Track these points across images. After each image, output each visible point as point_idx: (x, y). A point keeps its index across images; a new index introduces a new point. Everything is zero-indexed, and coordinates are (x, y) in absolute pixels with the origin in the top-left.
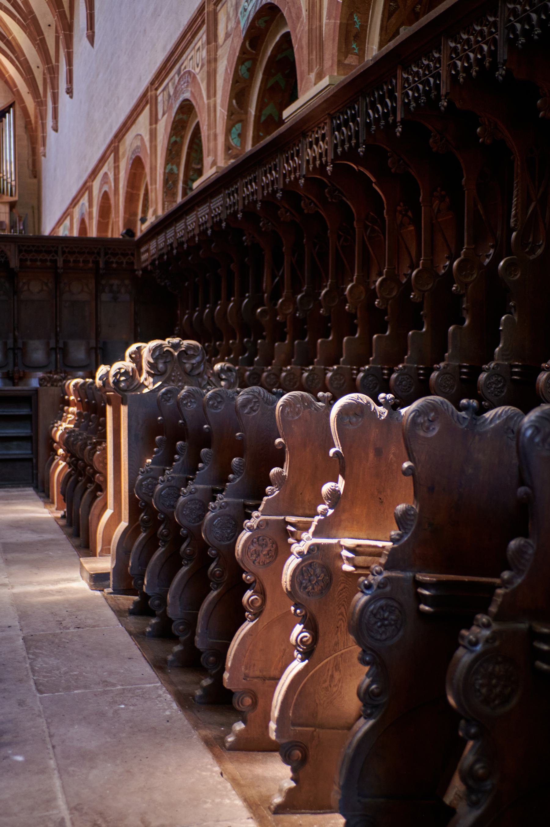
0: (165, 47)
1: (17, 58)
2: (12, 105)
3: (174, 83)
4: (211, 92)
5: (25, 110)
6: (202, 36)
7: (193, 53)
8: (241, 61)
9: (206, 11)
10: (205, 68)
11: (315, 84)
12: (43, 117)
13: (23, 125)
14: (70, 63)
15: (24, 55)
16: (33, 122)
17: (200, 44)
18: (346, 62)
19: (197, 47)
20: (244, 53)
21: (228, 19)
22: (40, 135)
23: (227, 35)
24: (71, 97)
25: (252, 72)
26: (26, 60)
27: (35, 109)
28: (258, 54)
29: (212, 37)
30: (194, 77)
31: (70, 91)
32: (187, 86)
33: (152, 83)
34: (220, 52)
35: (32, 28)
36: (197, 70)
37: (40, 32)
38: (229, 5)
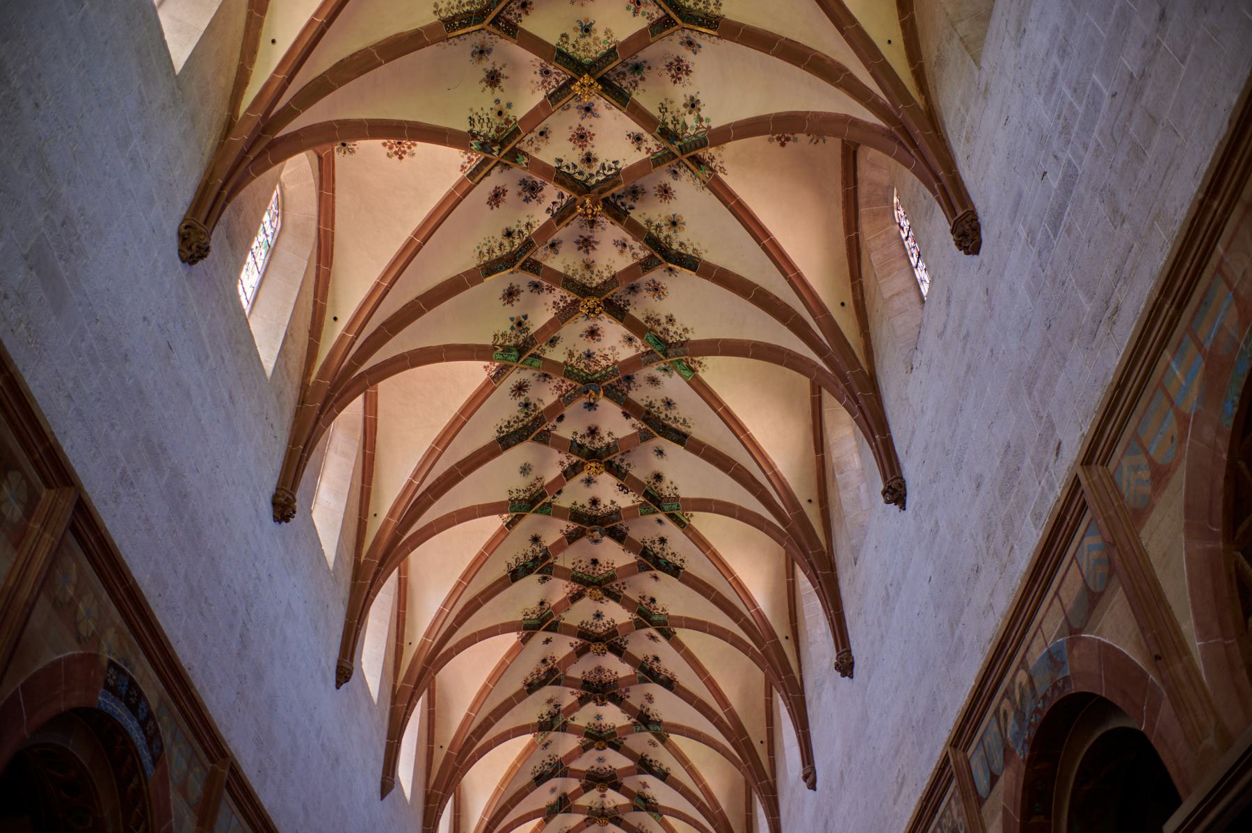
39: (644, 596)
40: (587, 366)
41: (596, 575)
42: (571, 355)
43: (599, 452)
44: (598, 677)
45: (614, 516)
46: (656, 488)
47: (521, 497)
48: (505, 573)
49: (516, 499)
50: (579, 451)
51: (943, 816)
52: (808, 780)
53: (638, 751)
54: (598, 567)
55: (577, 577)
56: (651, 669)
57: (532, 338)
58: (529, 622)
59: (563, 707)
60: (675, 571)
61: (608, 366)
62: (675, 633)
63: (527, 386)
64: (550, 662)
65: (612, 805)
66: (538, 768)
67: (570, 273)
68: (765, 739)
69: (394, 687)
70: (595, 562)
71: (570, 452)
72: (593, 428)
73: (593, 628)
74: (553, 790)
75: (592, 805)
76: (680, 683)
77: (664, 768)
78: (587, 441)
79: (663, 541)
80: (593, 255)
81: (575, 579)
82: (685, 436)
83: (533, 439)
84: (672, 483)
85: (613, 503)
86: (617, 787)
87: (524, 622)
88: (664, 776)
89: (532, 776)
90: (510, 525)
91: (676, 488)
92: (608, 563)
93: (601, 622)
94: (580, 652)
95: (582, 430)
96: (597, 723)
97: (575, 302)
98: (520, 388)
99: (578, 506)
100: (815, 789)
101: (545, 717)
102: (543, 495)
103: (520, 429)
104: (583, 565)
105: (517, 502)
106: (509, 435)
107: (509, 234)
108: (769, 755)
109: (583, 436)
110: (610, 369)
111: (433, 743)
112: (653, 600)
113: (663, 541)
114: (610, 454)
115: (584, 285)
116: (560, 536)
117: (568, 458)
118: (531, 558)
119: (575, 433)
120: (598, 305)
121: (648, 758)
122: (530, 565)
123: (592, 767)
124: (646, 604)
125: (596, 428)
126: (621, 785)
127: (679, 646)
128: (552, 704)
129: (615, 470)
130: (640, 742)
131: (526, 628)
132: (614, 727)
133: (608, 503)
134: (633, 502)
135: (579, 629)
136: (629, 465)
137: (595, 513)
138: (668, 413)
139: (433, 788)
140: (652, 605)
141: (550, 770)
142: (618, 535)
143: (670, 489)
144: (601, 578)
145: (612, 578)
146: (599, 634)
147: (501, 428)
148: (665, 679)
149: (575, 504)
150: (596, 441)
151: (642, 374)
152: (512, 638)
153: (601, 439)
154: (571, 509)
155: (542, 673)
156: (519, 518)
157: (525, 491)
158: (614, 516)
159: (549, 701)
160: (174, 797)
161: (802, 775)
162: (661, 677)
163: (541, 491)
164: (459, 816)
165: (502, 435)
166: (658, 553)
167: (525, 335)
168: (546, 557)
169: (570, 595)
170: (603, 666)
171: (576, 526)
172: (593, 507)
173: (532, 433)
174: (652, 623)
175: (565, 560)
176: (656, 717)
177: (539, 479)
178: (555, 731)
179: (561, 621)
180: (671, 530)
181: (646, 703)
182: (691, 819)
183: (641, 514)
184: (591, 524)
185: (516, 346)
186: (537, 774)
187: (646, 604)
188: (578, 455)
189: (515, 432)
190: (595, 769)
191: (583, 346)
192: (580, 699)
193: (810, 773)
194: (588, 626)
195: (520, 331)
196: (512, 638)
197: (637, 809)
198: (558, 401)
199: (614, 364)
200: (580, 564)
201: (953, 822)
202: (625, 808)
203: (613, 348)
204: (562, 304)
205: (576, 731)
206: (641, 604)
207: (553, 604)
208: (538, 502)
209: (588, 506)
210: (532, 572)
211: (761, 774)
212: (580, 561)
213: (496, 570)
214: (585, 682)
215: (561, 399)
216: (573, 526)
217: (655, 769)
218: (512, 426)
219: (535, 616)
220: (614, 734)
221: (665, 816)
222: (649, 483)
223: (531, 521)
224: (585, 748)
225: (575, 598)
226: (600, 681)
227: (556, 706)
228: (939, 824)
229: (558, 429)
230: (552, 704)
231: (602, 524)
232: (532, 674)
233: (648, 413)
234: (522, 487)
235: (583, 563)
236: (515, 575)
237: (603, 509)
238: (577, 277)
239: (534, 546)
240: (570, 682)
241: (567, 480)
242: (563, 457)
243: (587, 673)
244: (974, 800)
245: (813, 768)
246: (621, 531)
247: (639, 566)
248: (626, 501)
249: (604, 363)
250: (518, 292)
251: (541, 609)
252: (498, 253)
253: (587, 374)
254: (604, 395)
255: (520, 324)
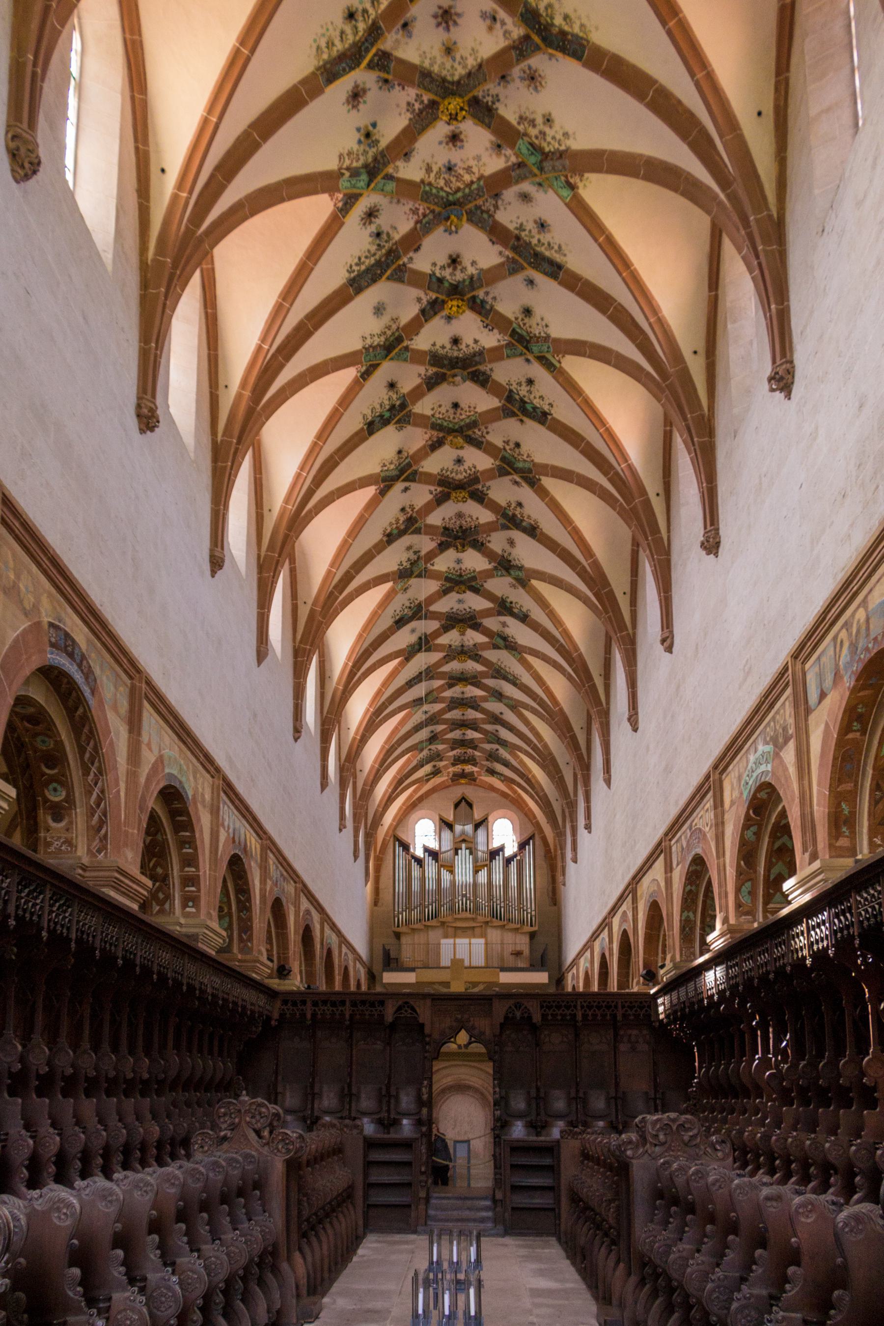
0: (677, 802)
1: (535, 793)
2: (532, 837)
3: (686, 837)
4: (720, 852)
5: (544, 839)
6: (709, 802)
7: (702, 813)
8: (746, 827)
9: (711, 779)
10: (714, 828)
11: (810, 864)
12: (563, 848)
13: (543, 853)
14: (588, 799)
15: (543, 790)
16: (552, 851)
17: (708, 805)
18: (838, 844)
19: (706, 808)
20: (748, 820)
21: (732, 789)
22: (559, 864)
23: (732, 803)
24: (590, 832)
25: (758, 835)
26: (545, 795)
27: (555, 840)
28: (762, 820)
29: (719, 803)
30: (705, 835)
31: (588, 827)
32: (699, 842)
33: (666, 834)
34: (726, 816)
35: (551, 768)
36: (707, 829)
37: (558, 770)
38: (732, 774)
39: (508, 441)
40: (448, 182)
41: (456, 420)
42: (429, 169)
43: (461, 286)
44: (458, 523)
45: (477, 358)
46: (524, 324)
47: (376, 343)
48: (361, 425)
49: (371, 346)
50: (439, 287)
51: (777, 713)
52: (665, 644)
53: (499, 594)
54: (459, 411)
55: (437, 425)
56: (514, 515)
57: (382, 154)
58: (388, 474)
59: (423, 553)
60: (542, 417)
61: (472, 182)
62: (540, 480)
63: (378, 211)
64: (409, 510)
65: (471, 643)
66: (398, 612)
67: (427, 64)
68: (628, 590)
69: (259, 556)
70: (456, 406)
71: (429, 289)
72: (454, 256)
73: (454, 475)
74: (413, 631)
75: (452, 643)
76: (544, 530)
77: (524, 610)
78: (447, 273)
79: (530, 382)
80: (456, 34)
81: (435, 427)
82: (559, 267)
83: (388, 279)
84: (542, 319)
85: (476, 341)
86: (476, 627)
87: (383, 474)
88: (524, 618)
89: (393, 620)
90: (366, 375)
91: (547, 326)
92: (469, 407)
93: (462, 468)
94: (440, 500)
95: (443, 260)
96: (457, 567)
97: (433, 104)
98: (371, 214)
99: (437, 347)
100: (671, 652)
101: (405, 564)
102: (399, 340)
103: (373, 266)
104: (443, 410)
105: (371, 350)
106: (360, 275)
107: (351, 16)
108: (631, 606)
109: (443, 268)
110: (475, 186)
111: (296, 599)
112: (518, 445)
113: (530, 382)
114: (473, 289)
115: (444, 80)
116: (418, 381)
117: (426, 294)
118: (388, 407)
119: (434, 264)
120: (462, 109)
121: (509, 600)
122: (387, 415)
123: (452, 608)
124: (510, 450)
125: (458, 256)
126: (480, 624)
127: (543, 493)
128: (411, 551)
129: (480, 308)
130: (500, 586)
131: (384, 480)
132: (474, 571)
133: (470, 342)
134: (499, 341)
135: (439, 477)
136: (494, 298)
137: (456, 354)
138: (541, 237)
139: (301, 642)
140: (517, 450)
141: (410, 614)
142: (481, 378)
143: (540, 327)
144: (462, 423)
145: (474, 424)
146: (460, 481)
147: (351, 266)
148: (528, 526)
149: (434, 345)
150: (458, 273)
151: (509, 194)
152: (370, 491)
153: (463, 270)
154: (430, 352)
155: (401, 522)
156: (375, 367)
157: (379, 336)
158: (477, 358)
159: (409, 548)
160: (111, 715)
161: (659, 638)
162: (524, 524)
163: (397, 334)
164: (324, 661)
165: (352, 275)
166: (524, 396)
167: (374, 150)
168: (403, 406)
169: (430, 443)
170: (464, 511)
171: (435, 369)
172: (455, 348)
173: (386, 271)
174: (517, 471)
175: (424, 407)
176: (517, 562)
177: (394, 320)
178: (416, 577)
179: (421, 470)
180: (537, 371)
181: (507, 547)
182: (550, 658)
183: (508, 357)
184: (453, 368)
185: (366, 166)
186: (397, 618)
187: (510, 450)
188: (438, 292)
189: (368, 270)
190: (454, 610)
191: (443, 156)
192: (440, 545)
193: (668, 637)
194: (449, 473)
195: (369, 146)
196: (370, 491)
197: (496, 647)
198: (415, 228)
199: (479, 179)
200: (440, 409)
201: (785, 720)
202: (484, 646)
203: (478, 158)
204: (417, 106)
205: (435, 575)
206: (505, 449)
207: (411, 452)
208: (394, 348)
209: (448, 346)
210: (389, 423)
211: (620, 625)
212: (440, 406)
213: (351, 423)
214: (446, 528)
215: (419, 226)
216: (432, 370)
217: (516, 611)
218: (364, 263)
219: (392, 467)
220: (474, 578)
221: (525, 655)
222: (516, 319)
223: (387, 369)
224: (445, 592)
225: (435, 445)
226: (461, 527)
227: (415, 553)
228: (774, 718)
229: (415, 261)
230: (411, 551)
231: (464, 368)
232: (391, 524)
233: (518, 238)
234: (377, 330)
235: (443, 407)
236: (371, 428)
237: (465, 349)
238: (436, 69)
239: (391, 393)
240: (430, 530)
241: (426, 321)
242: (421, 294)
243: (447, 519)
244: (802, 709)
245: (672, 632)
246: (484, 373)
247: (503, 411)
248: (491, 340)
249: (467, 178)
250: (364, 91)
251: (399, 458)
252: (339, 47)
253: (448, 194)
254: (468, 220)
255: (368, 135)
